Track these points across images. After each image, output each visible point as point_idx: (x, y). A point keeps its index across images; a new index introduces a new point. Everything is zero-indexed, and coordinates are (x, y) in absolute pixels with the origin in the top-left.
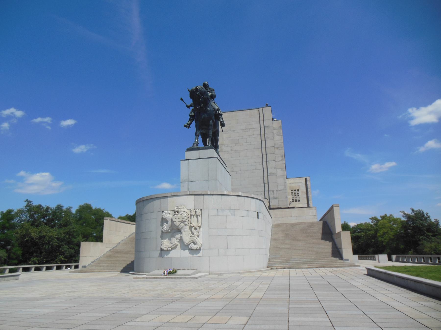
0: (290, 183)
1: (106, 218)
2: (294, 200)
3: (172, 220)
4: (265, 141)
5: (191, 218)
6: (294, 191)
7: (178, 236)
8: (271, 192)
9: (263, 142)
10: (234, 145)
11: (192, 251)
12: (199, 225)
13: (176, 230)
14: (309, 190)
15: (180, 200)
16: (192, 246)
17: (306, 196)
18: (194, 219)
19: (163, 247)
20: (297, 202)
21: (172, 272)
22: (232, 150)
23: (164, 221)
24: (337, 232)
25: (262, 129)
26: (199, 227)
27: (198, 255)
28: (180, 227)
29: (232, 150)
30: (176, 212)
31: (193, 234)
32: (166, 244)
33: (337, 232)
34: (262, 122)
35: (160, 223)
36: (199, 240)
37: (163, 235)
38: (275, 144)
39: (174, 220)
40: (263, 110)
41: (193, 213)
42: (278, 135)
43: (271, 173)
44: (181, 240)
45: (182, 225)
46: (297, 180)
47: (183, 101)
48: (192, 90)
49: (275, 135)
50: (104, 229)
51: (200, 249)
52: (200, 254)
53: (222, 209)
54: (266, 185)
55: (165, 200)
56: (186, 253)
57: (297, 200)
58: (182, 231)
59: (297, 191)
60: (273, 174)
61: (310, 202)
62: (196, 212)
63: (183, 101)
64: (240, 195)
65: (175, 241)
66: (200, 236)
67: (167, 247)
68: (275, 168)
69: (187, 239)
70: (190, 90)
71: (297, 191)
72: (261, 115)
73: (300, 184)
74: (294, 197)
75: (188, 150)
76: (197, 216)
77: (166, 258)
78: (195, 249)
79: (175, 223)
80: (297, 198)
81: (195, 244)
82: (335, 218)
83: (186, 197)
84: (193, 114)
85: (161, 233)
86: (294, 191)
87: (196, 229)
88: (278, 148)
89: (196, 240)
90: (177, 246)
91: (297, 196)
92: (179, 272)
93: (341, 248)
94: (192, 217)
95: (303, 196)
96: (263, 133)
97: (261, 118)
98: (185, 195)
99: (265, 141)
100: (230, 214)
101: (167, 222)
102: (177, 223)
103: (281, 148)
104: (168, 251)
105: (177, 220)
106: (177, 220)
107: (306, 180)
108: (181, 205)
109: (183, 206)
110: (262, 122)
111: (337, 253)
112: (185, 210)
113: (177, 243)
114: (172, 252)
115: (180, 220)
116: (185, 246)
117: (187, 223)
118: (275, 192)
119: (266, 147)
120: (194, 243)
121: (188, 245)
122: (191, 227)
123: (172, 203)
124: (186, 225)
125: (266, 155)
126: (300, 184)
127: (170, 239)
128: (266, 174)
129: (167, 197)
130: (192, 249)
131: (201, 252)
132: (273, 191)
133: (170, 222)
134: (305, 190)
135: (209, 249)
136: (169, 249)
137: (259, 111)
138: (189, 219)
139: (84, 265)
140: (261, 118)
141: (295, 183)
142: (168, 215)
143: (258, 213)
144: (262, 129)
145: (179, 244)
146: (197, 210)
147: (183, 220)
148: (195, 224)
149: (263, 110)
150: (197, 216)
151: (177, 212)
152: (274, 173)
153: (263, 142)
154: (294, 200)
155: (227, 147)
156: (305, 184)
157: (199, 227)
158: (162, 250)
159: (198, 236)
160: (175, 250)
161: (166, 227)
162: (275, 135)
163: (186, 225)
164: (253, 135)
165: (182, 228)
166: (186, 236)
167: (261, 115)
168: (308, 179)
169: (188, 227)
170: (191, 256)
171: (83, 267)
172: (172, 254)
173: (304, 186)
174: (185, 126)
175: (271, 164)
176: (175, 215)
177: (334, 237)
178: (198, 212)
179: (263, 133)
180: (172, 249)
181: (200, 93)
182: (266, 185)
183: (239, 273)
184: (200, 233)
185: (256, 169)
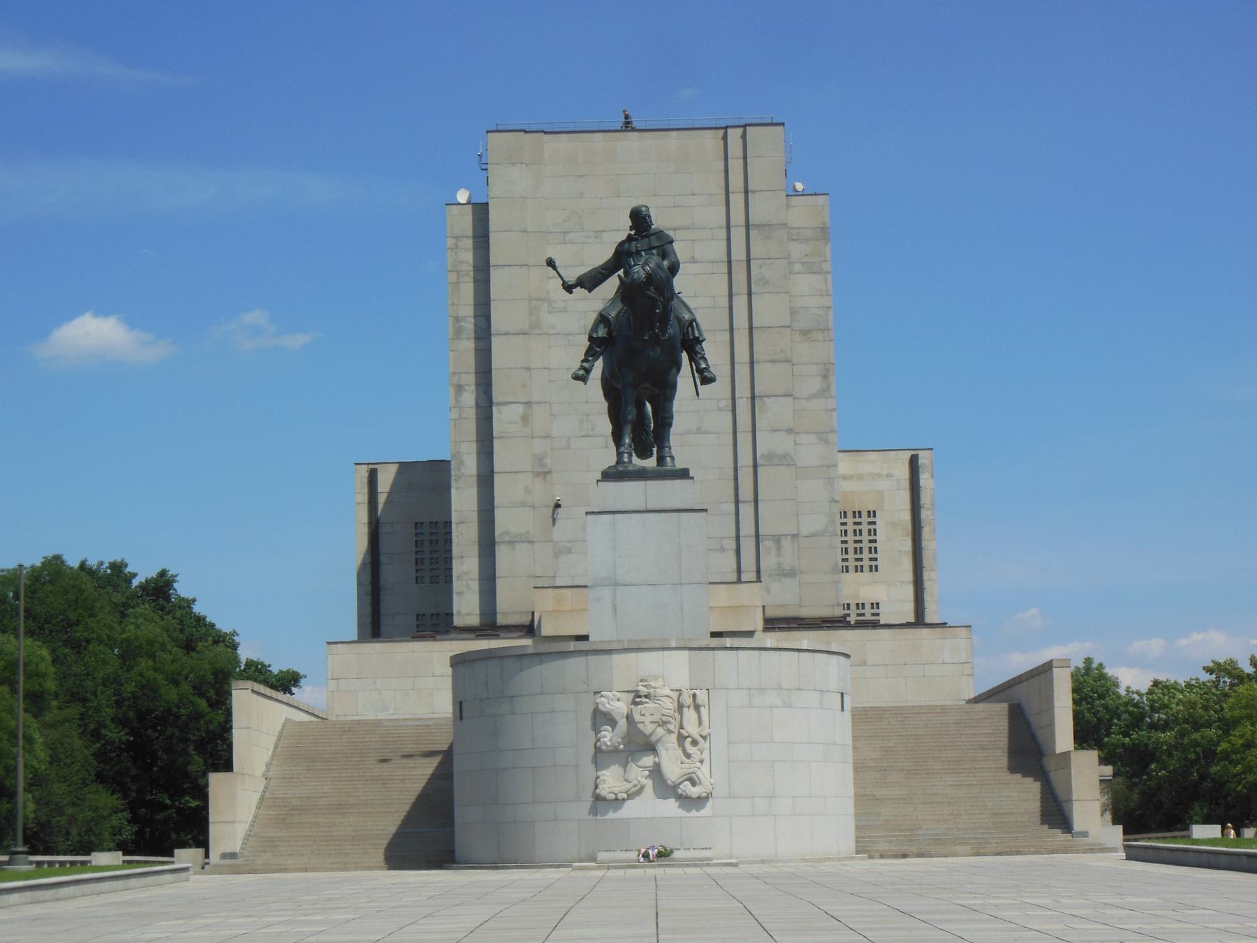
1: (241, 684)
2: (851, 564)
3: (629, 717)
4: (750, 294)
5: (681, 713)
7: (648, 760)
8: (766, 545)
9: (740, 302)
11: (689, 802)
12: (704, 733)
13: (639, 744)
15: (649, 663)
16: (686, 788)
17: (908, 545)
18: (689, 715)
19: (604, 790)
20: (866, 575)
21: (664, 854)
23: (601, 718)
24: (1059, 750)
25: (738, 235)
26: (704, 738)
27: (703, 813)
28: (653, 738)
30: (637, 698)
31: (688, 756)
32: (611, 780)
33: (1059, 750)
34: (737, 200)
35: (589, 723)
36: (703, 773)
37: (601, 757)
38: (793, 312)
39: (637, 718)
40: (744, 136)
41: (687, 699)
42: (812, 269)
43: (771, 456)
44: (656, 772)
45: (661, 731)
46: (870, 463)
47: (554, 268)
49: (798, 267)
50: (235, 724)
51: (707, 798)
52: (707, 810)
53: (762, 690)
54: (747, 511)
55: (603, 658)
56: (670, 807)
57: (866, 563)
58: (660, 747)
59: (865, 519)
60: (785, 460)
62: (694, 696)
63: (554, 268)
64: (805, 647)
65: (639, 772)
66: (707, 762)
67: (616, 790)
68: (790, 431)
69: (673, 769)
71: (865, 519)
72: (736, 166)
73: (885, 485)
76: (697, 708)
77: (612, 820)
78: (695, 796)
79: (640, 726)
80: (866, 555)
81: (694, 784)
82: (1056, 704)
83: (666, 653)
84: (602, 333)
85: (592, 751)
87: (695, 743)
88: (805, 333)
89: (699, 773)
90: (642, 788)
91: (865, 545)
92: (676, 855)
93: (1070, 801)
94: (685, 710)
96: (739, 253)
97: (736, 181)
98: (663, 649)
99: (750, 294)
100: (780, 703)
101: (612, 722)
102: (648, 728)
103: (820, 336)
104: (617, 802)
105: (647, 719)
106: (647, 719)
108: (656, 678)
109: (660, 683)
110: (737, 200)
111: (1056, 814)
112: (667, 691)
113: (644, 781)
114: (628, 803)
115: (657, 717)
116: (665, 788)
117: (671, 727)
118: (787, 544)
119: (751, 329)
121: (675, 787)
122: (681, 739)
123: (626, 670)
124: (670, 732)
125: (752, 363)
126: (885, 485)
127: (625, 766)
128: (745, 459)
130: (688, 798)
131: (709, 804)
132: (777, 539)
133: (622, 724)
134: (906, 516)
135: (730, 797)
136: (621, 796)
137: (725, 138)
138: (677, 715)
139: (228, 850)
140: (736, 181)
141: (860, 477)
142: (617, 705)
144: (738, 235)
145: (649, 783)
146: (698, 692)
147: (664, 719)
148: (691, 728)
149: (744, 136)
150: (697, 708)
152: (785, 456)
153: (740, 302)
155: (564, 310)
156: (906, 484)
157: (704, 738)
158: (598, 798)
159: (701, 762)
160: (637, 799)
161: (608, 737)
162: (798, 267)
163: (670, 732)
165: (659, 740)
166: (672, 763)
167: (736, 166)
168: (924, 458)
169: (674, 737)
170: (684, 813)
171: (224, 856)
172: (630, 810)
173: (905, 495)
174: (576, 377)
175: (774, 412)
177: (1049, 764)
178: (702, 696)
179: (739, 253)
180: (631, 796)
182: (747, 511)
183: (804, 860)
184: (706, 755)
185: (699, 431)
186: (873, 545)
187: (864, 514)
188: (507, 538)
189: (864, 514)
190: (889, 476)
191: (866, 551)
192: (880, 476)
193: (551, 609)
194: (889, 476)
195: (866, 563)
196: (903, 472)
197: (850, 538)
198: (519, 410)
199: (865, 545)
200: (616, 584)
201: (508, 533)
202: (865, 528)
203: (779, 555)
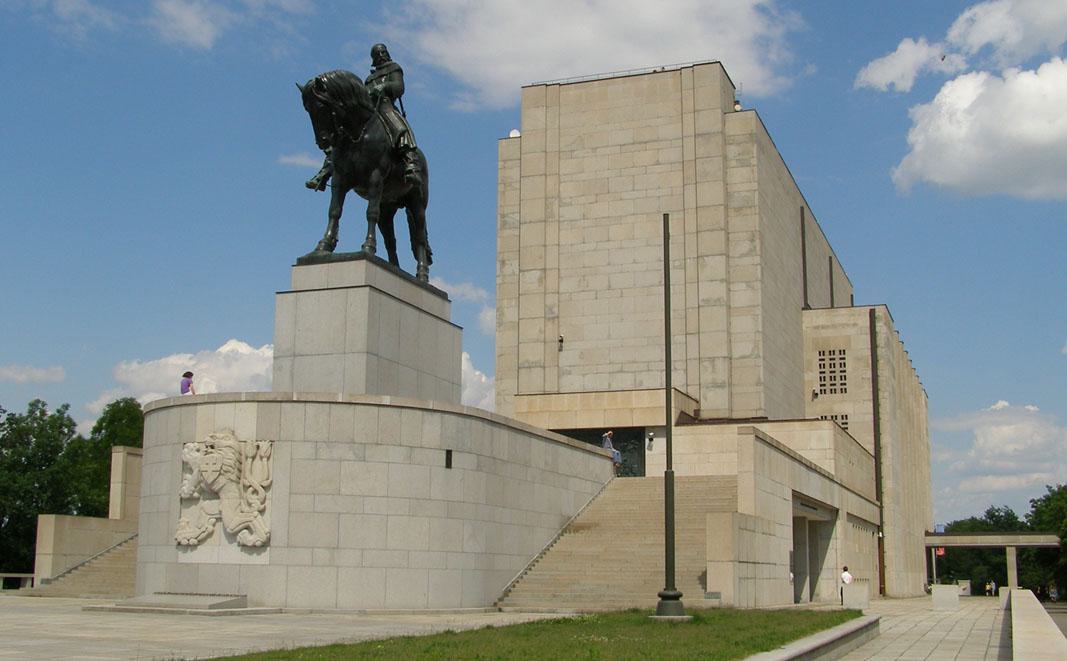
0: (817, 328)
2: (828, 388)
6: (827, 357)
10: (592, 198)
14: (880, 351)
17: (869, 374)
22: (584, 217)
28: (216, 487)
29: (584, 217)
42: (743, 164)
48: (307, 86)
58: (221, 495)
59: (837, 356)
61: (881, 394)
67: (188, 536)
70: (303, 85)
71: (837, 356)
73: (851, 331)
74: (827, 375)
75: (302, 262)
78: (250, 544)
81: (251, 532)
86: (827, 357)
91: (838, 375)
95: (857, 371)
101: (191, 471)
103: (749, 211)
107: (872, 313)
120: (248, 528)
126: (851, 331)
129: (196, 404)
141: (834, 326)
142: (191, 454)
143: (449, 453)
151: (212, 447)
154: (828, 388)
159: (262, 512)
164: (658, 163)
168: (880, 312)
174: (310, 186)
176: (207, 453)
181: (332, 95)
186: (843, 374)
187: (837, 353)
188: (526, 365)
189: (837, 353)
190: (855, 325)
191: (838, 378)
192: (848, 325)
193: (525, 410)
194: (855, 325)
195: (838, 387)
196: (865, 321)
197: (827, 369)
198: (538, 274)
199: (838, 375)
200: (295, 356)
201: (527, 361)
202: (837, 362)
203: (713, 372)
